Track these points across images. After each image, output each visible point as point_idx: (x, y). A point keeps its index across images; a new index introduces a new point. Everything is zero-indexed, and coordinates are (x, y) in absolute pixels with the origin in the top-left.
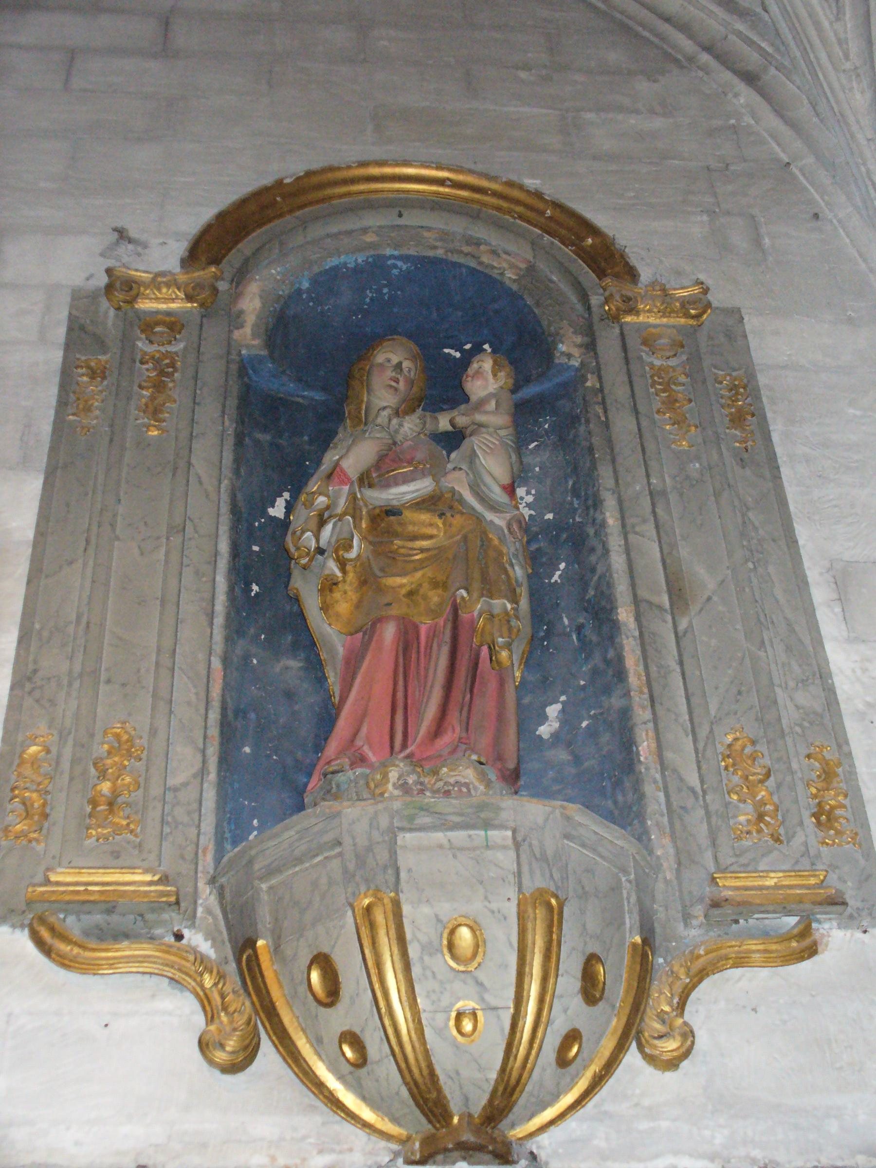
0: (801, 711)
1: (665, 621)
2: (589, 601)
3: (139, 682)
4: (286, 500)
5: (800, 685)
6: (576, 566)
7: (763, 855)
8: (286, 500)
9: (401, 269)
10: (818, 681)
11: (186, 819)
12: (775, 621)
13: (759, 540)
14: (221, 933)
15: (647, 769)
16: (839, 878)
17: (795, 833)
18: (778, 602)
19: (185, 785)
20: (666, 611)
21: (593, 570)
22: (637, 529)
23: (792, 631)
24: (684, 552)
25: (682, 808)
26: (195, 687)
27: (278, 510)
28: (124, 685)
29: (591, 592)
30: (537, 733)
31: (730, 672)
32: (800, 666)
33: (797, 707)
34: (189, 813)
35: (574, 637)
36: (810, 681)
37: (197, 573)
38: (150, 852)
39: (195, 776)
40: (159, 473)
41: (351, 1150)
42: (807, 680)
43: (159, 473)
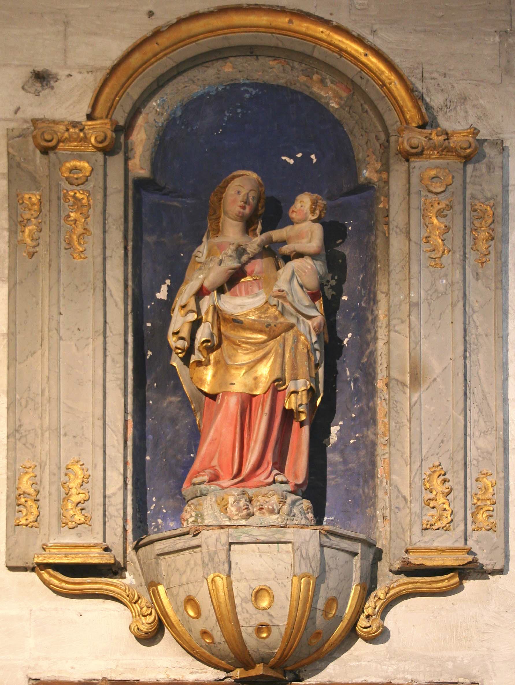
0: (479, 451)
1: (405, 393)
2: (363, 364)
3: (83, 435)
4: (168, 285)
5: (482, 434)
6: (358, 337)
7: (438, 537)
8: (168, 285)
9: (251, 94)
10: (494, 432)
11: (116, 514)
12: (475, 393)
13: (476, 335)
14: (138, 571)
15: (381, 482)
16: (480, 548)
17: (459, 525)
18: (480, 380)
19: (114, 494)
20: (406, 386)
21: (368, 345)
22: (397, 328)
23: (485, 398)
24: (425, 346)
25: (396, 508)
26: (116, 436)
27: (162, 294)
28: (75, 437)
29: (365, 360)
30: (324, 442)
31: (439, 428)
32: (485, 422)
33: (478, 449)
34: (117, 510)
35: (352, 385)
36: (489, 432)
37: (113, 360)
38: (98, 533)
39: (119, 489)
40: (84, 290)
41: (206, 672)
42: (487, 432)
43: (84, 290)
